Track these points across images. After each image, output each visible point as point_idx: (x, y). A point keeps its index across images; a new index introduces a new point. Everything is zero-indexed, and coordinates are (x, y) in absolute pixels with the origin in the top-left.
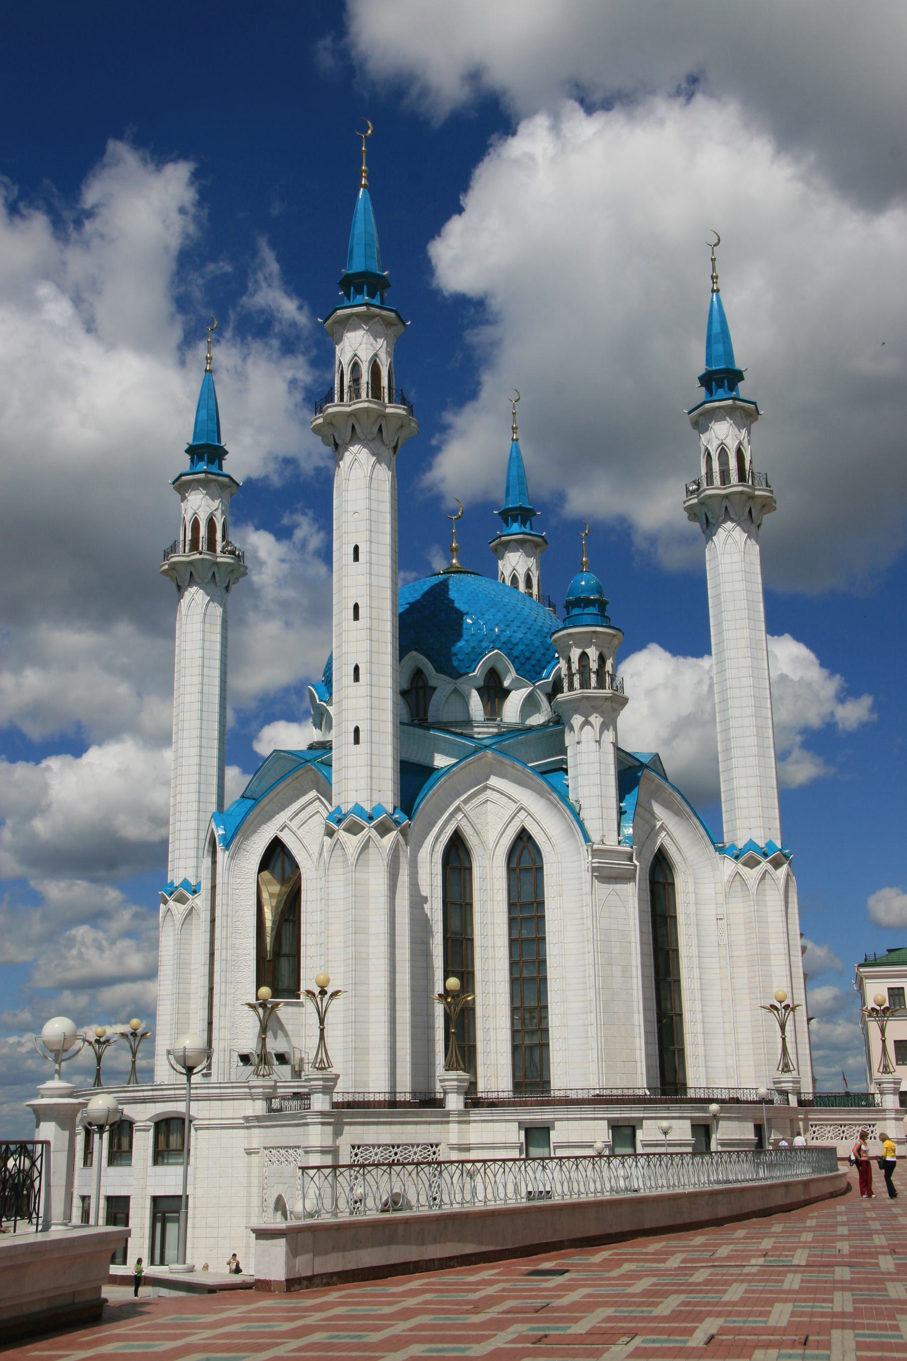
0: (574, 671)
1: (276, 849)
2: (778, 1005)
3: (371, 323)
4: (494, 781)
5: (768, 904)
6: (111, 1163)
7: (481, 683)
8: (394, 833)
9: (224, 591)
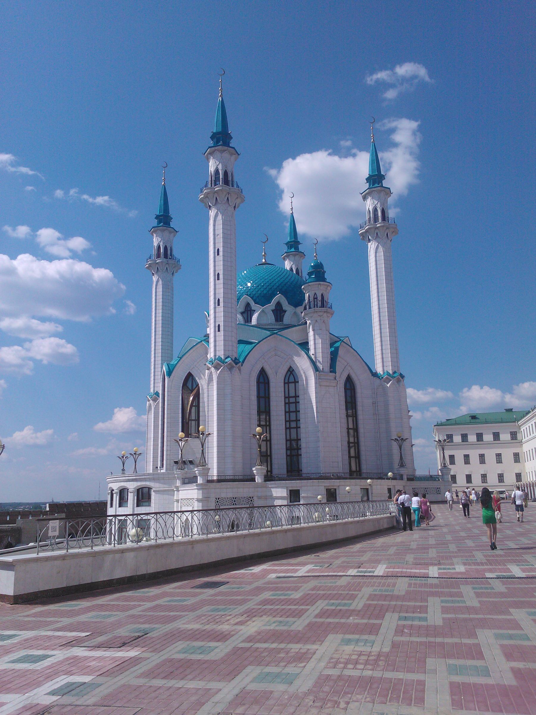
0: (311, 300)
1: (190, 376)
2: (398, 439)
6: (120, 506)
8: (235, 368)
9: (171, 275)
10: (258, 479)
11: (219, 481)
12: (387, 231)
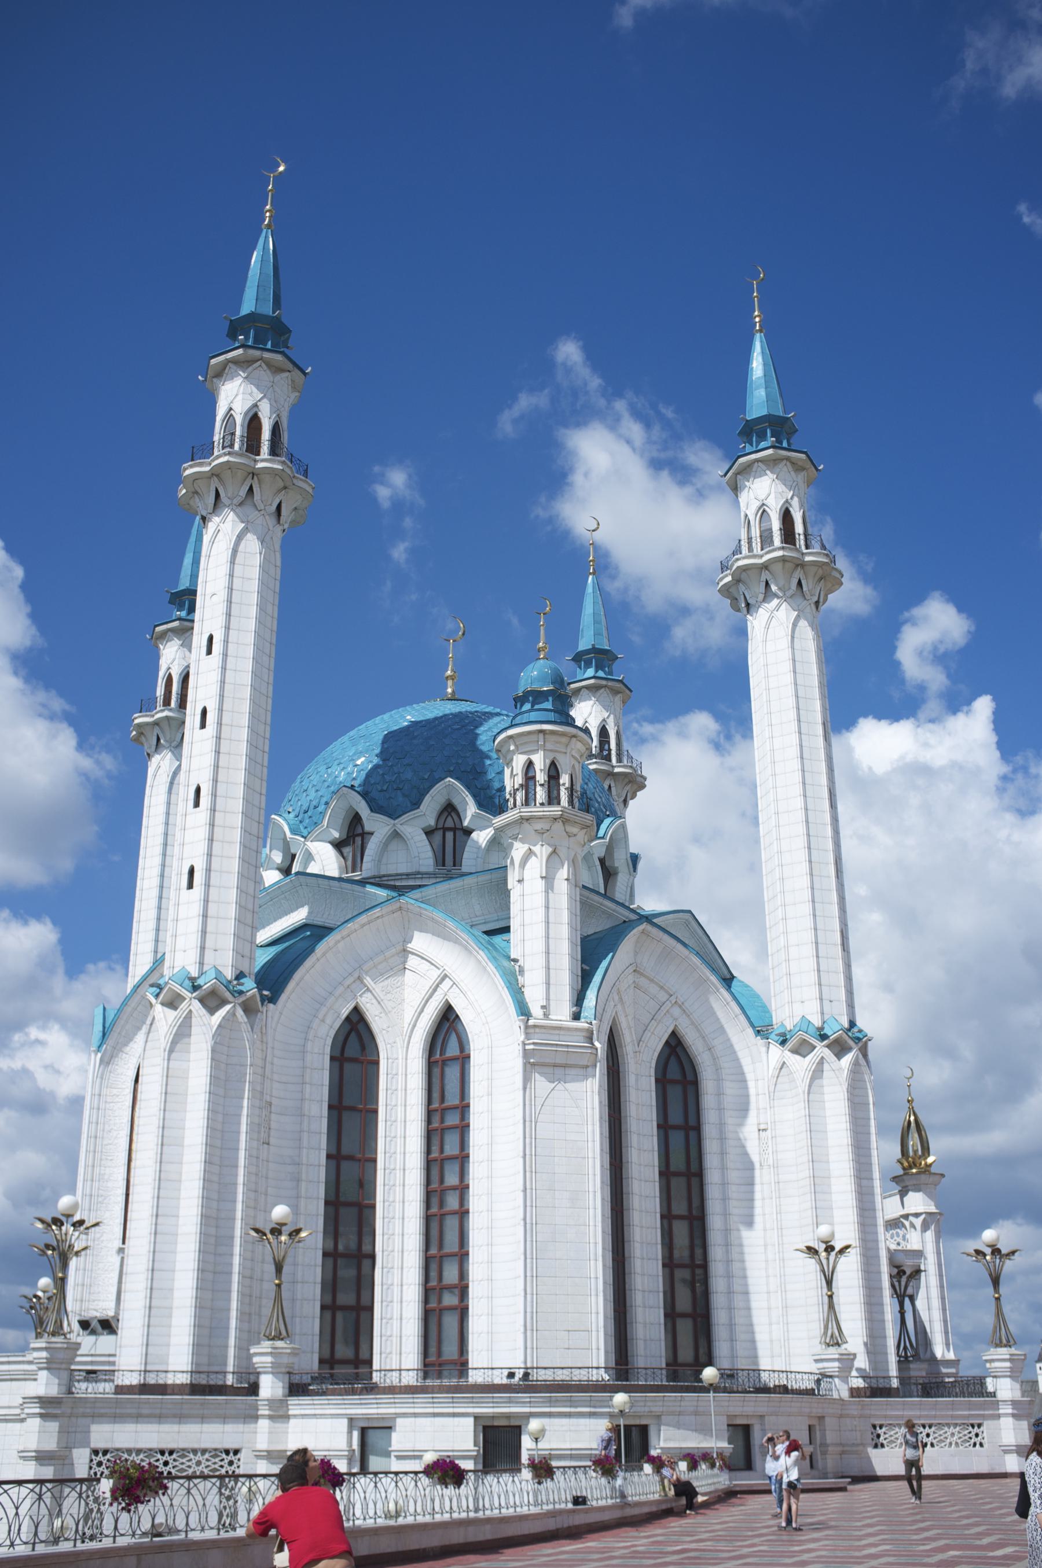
3: (250, 369)
4: (420, 942)
5: (827, 1105)
7: (432, 822)
10: (270, 1387)
11: (144, 1388)
12: (799, 573)
